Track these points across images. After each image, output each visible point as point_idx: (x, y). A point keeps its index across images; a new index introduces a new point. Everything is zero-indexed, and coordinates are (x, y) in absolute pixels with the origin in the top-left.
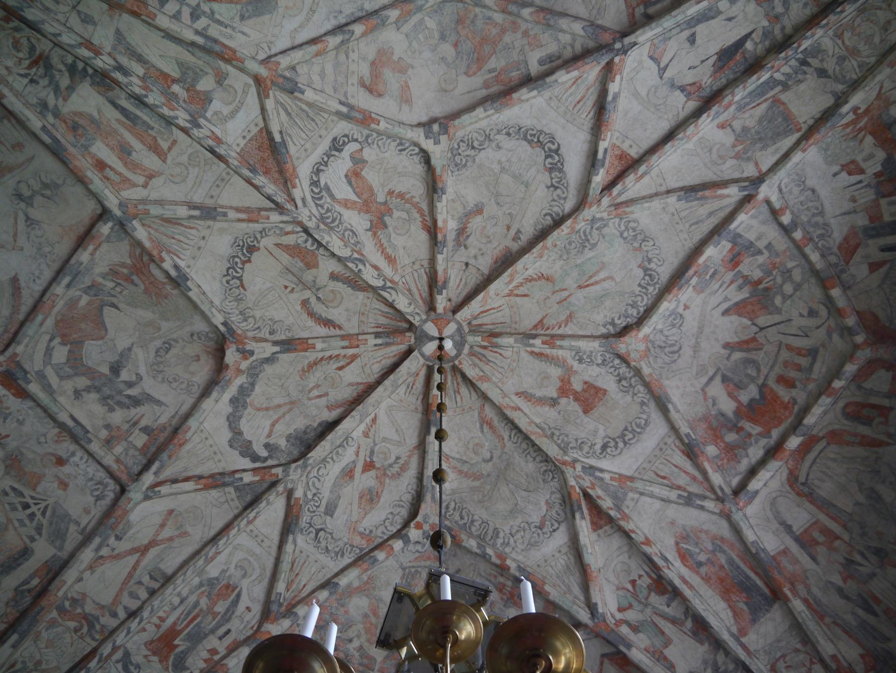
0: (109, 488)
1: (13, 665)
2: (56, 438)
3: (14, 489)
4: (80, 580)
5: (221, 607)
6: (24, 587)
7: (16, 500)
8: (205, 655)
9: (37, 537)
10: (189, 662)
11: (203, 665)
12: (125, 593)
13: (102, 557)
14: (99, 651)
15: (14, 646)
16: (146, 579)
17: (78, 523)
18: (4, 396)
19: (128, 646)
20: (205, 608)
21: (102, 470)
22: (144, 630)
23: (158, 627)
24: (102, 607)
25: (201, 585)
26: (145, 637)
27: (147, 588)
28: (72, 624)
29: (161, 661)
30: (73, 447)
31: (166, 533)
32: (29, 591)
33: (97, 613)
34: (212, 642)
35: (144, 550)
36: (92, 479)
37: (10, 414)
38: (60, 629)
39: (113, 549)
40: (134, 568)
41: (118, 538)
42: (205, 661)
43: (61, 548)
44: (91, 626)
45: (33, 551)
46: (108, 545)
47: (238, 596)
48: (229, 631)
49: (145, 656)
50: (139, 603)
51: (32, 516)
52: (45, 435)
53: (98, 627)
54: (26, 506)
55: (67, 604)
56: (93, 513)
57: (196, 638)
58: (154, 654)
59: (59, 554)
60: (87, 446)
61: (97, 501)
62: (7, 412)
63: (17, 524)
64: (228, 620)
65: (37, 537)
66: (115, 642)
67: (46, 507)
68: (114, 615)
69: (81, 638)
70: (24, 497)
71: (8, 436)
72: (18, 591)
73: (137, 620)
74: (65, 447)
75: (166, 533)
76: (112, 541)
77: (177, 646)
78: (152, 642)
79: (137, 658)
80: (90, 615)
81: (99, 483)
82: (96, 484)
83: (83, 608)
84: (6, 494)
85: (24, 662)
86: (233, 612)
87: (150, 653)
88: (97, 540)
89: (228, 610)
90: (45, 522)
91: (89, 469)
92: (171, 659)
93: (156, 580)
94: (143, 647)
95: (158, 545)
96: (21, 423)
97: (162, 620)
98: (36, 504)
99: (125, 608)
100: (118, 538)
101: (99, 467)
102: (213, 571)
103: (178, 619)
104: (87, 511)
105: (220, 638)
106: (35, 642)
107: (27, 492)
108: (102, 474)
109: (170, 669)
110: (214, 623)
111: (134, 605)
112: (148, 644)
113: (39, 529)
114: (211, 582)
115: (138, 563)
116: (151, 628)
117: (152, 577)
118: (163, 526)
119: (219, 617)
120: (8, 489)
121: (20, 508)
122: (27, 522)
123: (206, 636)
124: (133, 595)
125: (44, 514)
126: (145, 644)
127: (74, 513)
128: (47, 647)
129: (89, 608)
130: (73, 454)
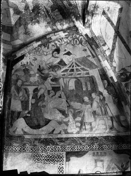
2: (46, 48)
3: (63, 71)
9: (87, 72)
18: (21, 63)
37: (30, 62)
41: (105, 44)
46: (106, 50)
54: (72, 70)
61: (81, 44)
62: (29, 63)
63: (79, 76)
67: (76, 64)
70: (68, 70)
71: (40, 66)
83: (128, 72)
84: (64, 75)
98: (73, 67)
100: (105, 44)
120: (63, 74)
121: (72, 73)
125: (78, 66)
127: (84, 54)
130: (56, 44)
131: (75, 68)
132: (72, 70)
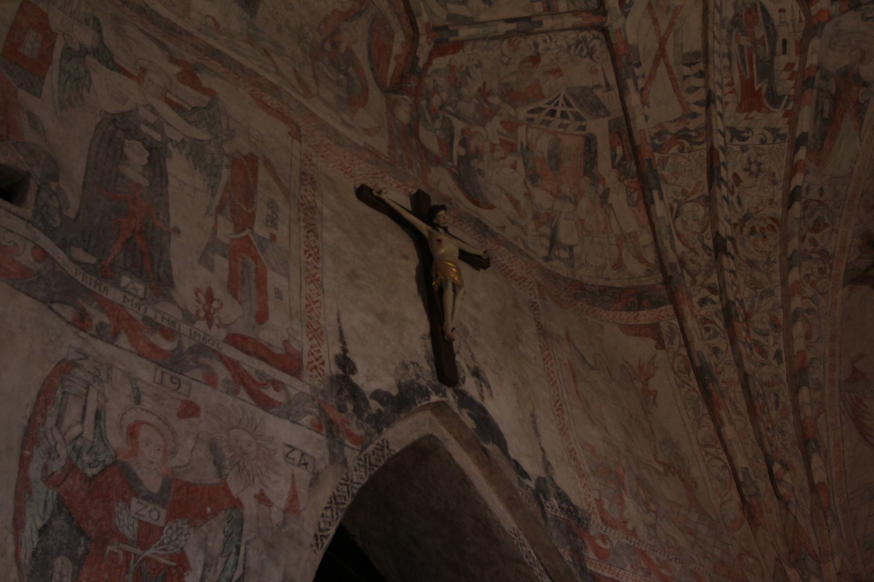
0: (589, 40)
1: (672, 209)
3: (531, 112)
4: (647, 118)
5: (760, 32)
6: (617, 160)
7: (542, 116)
8: (785, 75)
9: (583, 123)
10: (779, 90)
11: (791, 83)
12: (684, 95)
13: (643, 89)
14: (716, 146)
15: (661, 198)
16: (686, 71)
17: (598, 86)
18: (450, 61)
19: (728, 124)
20: (749, 44)
21: (568, 33)
22: (727, 103)
23: (733, 91)
24: (681, 119)
25: (730, 32)
26: (732, 107)
27: (695, 75)
28: (674, 149)
29: (760, 111)
30: (530, 40)
31: (664, 25)
32: (623, 159)
33: (681, 126)
34: (781, 61)
35: (662, 53)
36: (569, 47)
37: (467, 68)
38: (670, 160)
39: (643, 76)
40: (670, 72)
41: (638, 65)
42: (790, 78)
43: (608, 114)
44: (688, 138)
45: (592, 135)
47: (764, 9)
48: (785, 42)
49: (746, 118)
50: (703, 91)
51: (564, 115)
52: (503, 55)
53: (693, 134)
54: (553, 113)
55: (656, 141)
56: (600, 68)
57: (767, 70)
58: (750, 111)
59: (611, 118)
60: (541, 29)
61: (591, 57)
62: (464, 69)
63: (561, 130)
64: (776, 35)
65: (583, 123)
66: (719, 131)
67: (565, 99)
68: (695, 115)
69: (690, 151)
70: (544, 109)
71: (485, 84)
72: (618, 166)
73: (718, 102)
74: (525, 46)
75: (664, 25)
76: (637, 72)
77: (760, 89)
78: (740, 105)
79: (742, 125)
80: (680, 131)
81: (578, 43)
82: (577, 47)
84: (532, 120)
85: (675, 200)
86: (773, 25)
87: (745, 114)
88: (630, 82)
89: (767, 28)
90: (576, 109)
91: (559, 43)
92: (765, 101)
93: (694, 64)
94: (737, 114)
95: (666, 40)
96: (480, 65)
97: (731, 84)
98: (557, 105)
99: (696, 103)
100: (638, 65)
101: (564, 33)
102: (729, 13)
103: (740, 72)
104: (594, 72)
105: (784, 52)
106: (667, 183)
107: (542, 104)
108: (572, 36)
109: (772, 109)
110: (767, 47)
111: (701, 95)
112: (739, 109)
113: (578, 117)
114: (735, 22)
115: (668, 66)
116: (729, 98)
117: (689, 65)
118: (655, 22)
119: (766, 39)
120: (530, 116)
121: (551, 119)
122: (566, 121)
123: (772, 62)
124: (692, 90)
125: (569, 105)
126: (738, 111)
128: (677, 178)
129: (673, 129)
130: (536, 45)
131: (559, 109)
132: (553, 113)
